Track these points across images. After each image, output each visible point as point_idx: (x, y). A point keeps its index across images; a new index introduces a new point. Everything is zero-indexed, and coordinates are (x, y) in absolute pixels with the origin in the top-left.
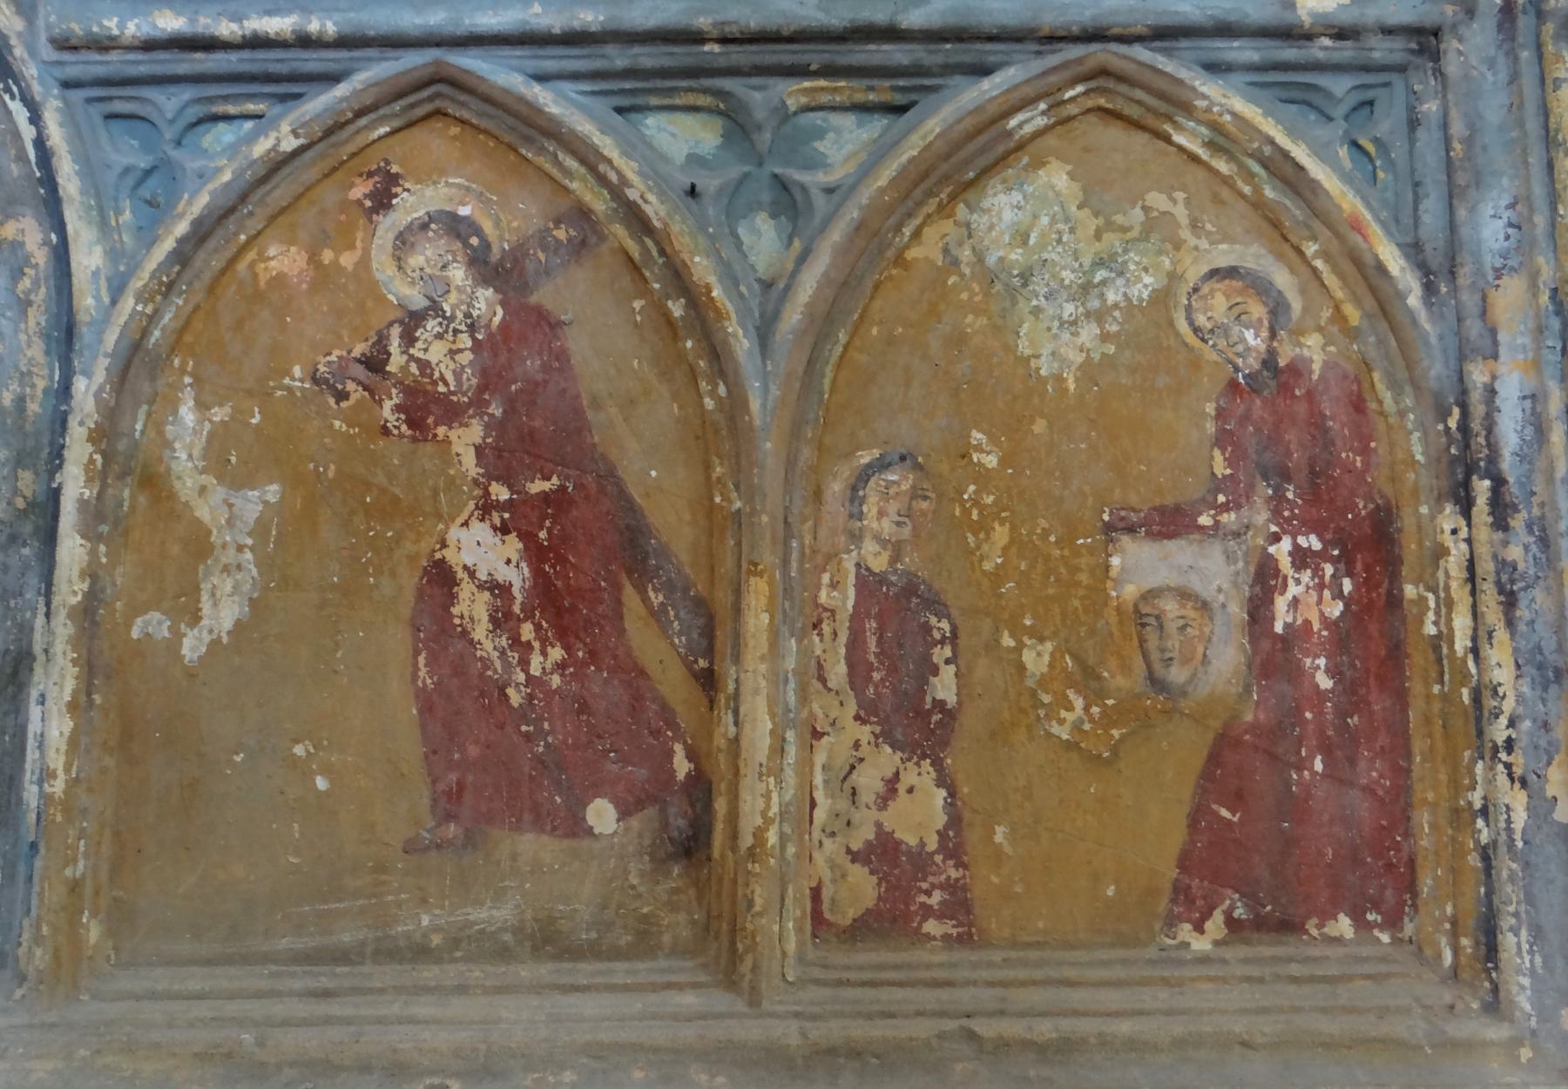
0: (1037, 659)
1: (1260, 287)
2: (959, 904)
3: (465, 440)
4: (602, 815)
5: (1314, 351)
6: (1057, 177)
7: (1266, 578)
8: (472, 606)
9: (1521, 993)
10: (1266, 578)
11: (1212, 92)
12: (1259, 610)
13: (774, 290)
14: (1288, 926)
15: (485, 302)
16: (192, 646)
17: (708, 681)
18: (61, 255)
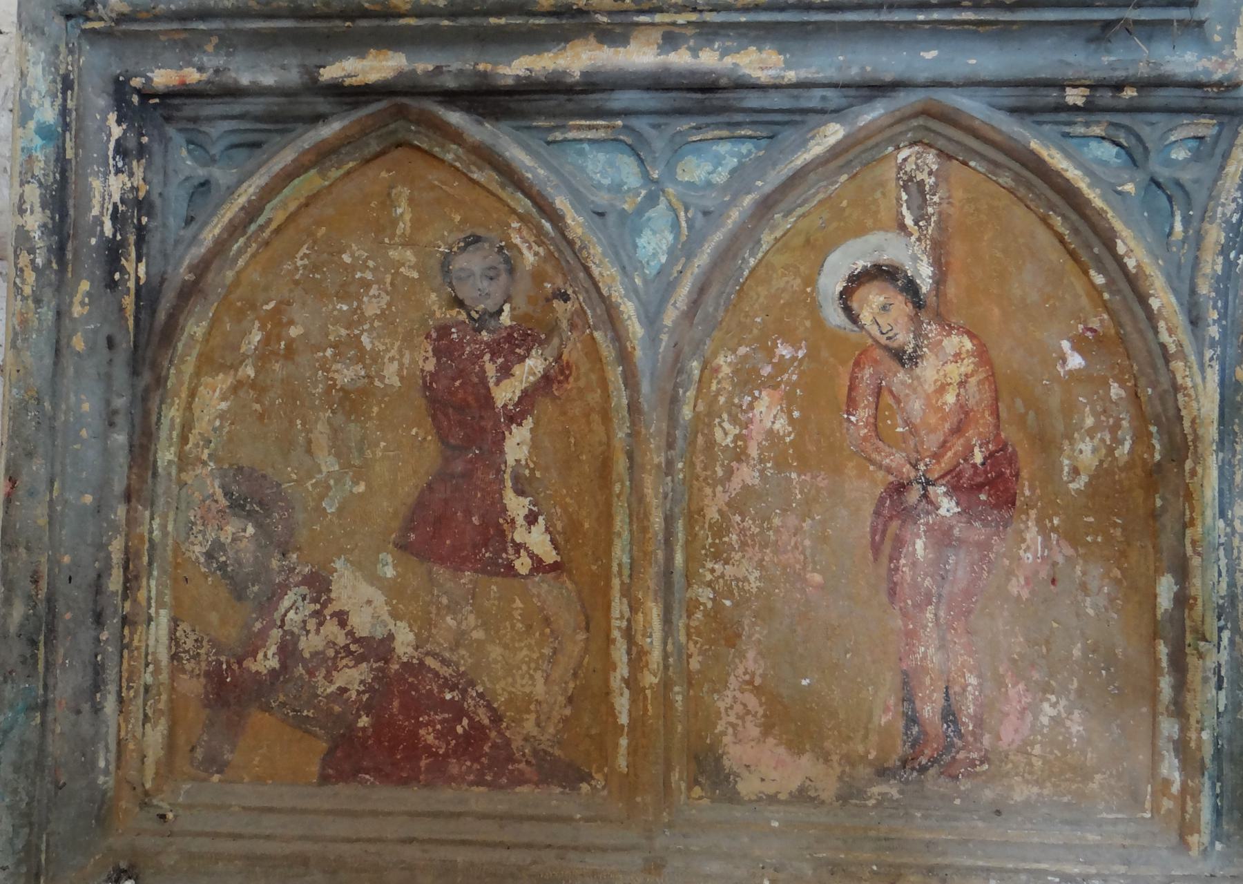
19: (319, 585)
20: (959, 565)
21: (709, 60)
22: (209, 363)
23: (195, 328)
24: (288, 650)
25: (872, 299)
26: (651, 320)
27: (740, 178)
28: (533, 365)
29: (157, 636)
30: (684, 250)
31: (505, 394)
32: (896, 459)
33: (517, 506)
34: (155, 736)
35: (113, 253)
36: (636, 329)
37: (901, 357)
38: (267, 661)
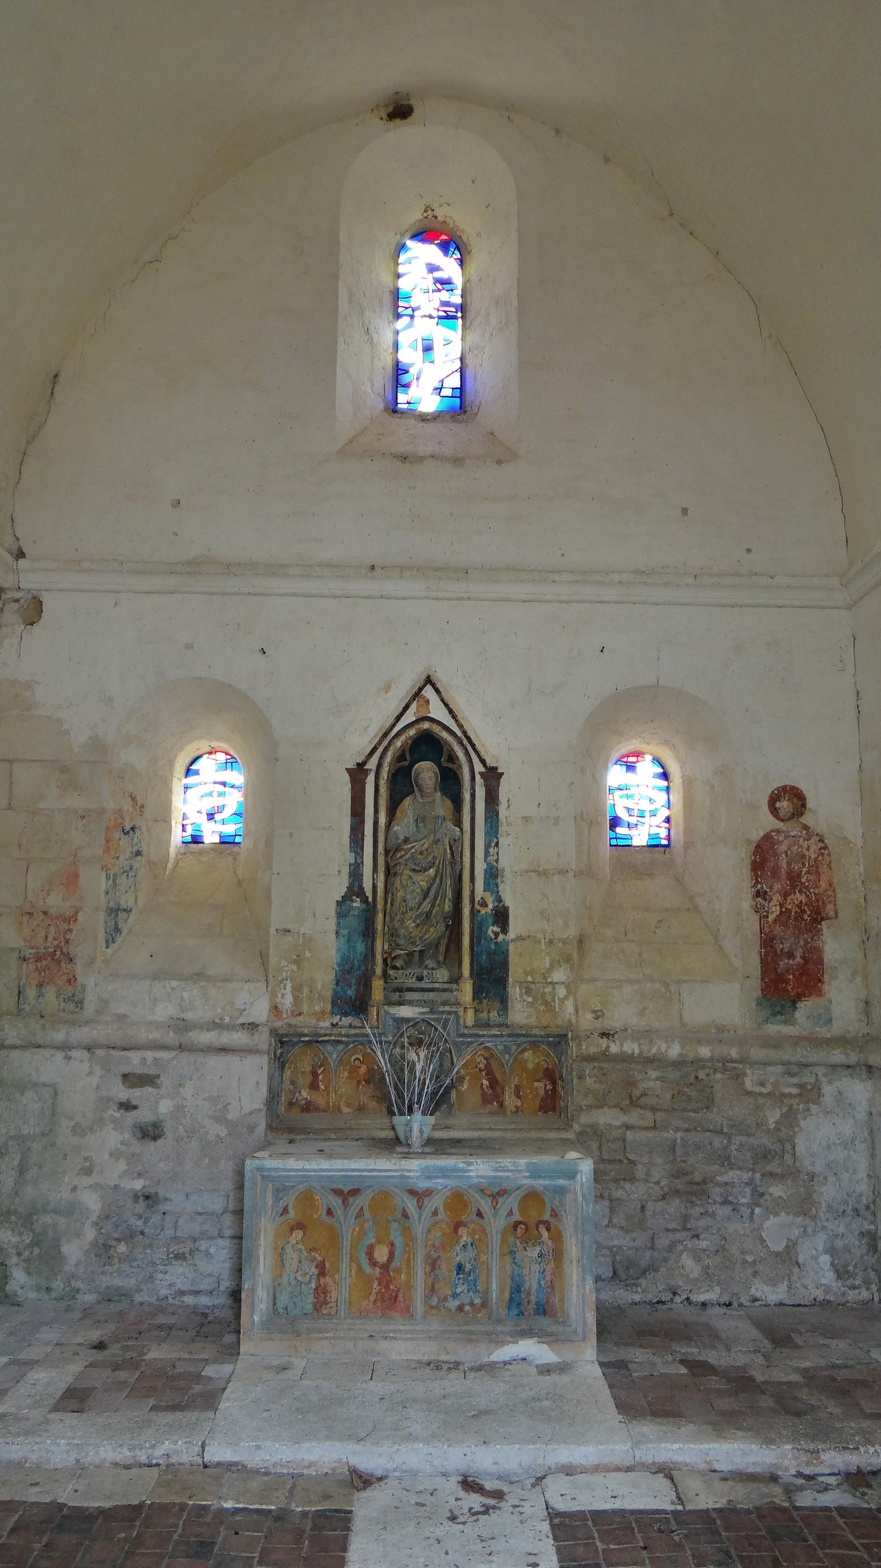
0: (528, 1091)
1: (546, 1061)
2: (522, 1111)
3: (484, 1073)
4: (495, 1103)
5: (550, 1067)
6: (531, 1051)
7: (546, 1085)
8: (484, 1087)
9: (562, 1117)
10: (546, 1085)
11: (542, 1046)
12: (545, 1088)
13: (508, 1061)
14: (547, 1112)
15: (485, 1062)
16: (463, 1089)
17: (503, 1093)
18: (452, 1057)
19: (300, 1092)
20: (365, 1089)
21: (339, 1038)
22: (289, 1068)
23: (287, 1065)
24: (297, 1099)
25: (357, 1061)
26: (334, 1064)
27: (344, 1049)
28: (322, 1068)
29: (283, 1098)
30: (337, 1057)
31: (319, 1072)
32: (358, 1078)
33: (321, 1083)
34: (283, 1109)
35: (279, 1058)
36: (332, 1065)
37: (359, 1067)
38: (294, 1101)
